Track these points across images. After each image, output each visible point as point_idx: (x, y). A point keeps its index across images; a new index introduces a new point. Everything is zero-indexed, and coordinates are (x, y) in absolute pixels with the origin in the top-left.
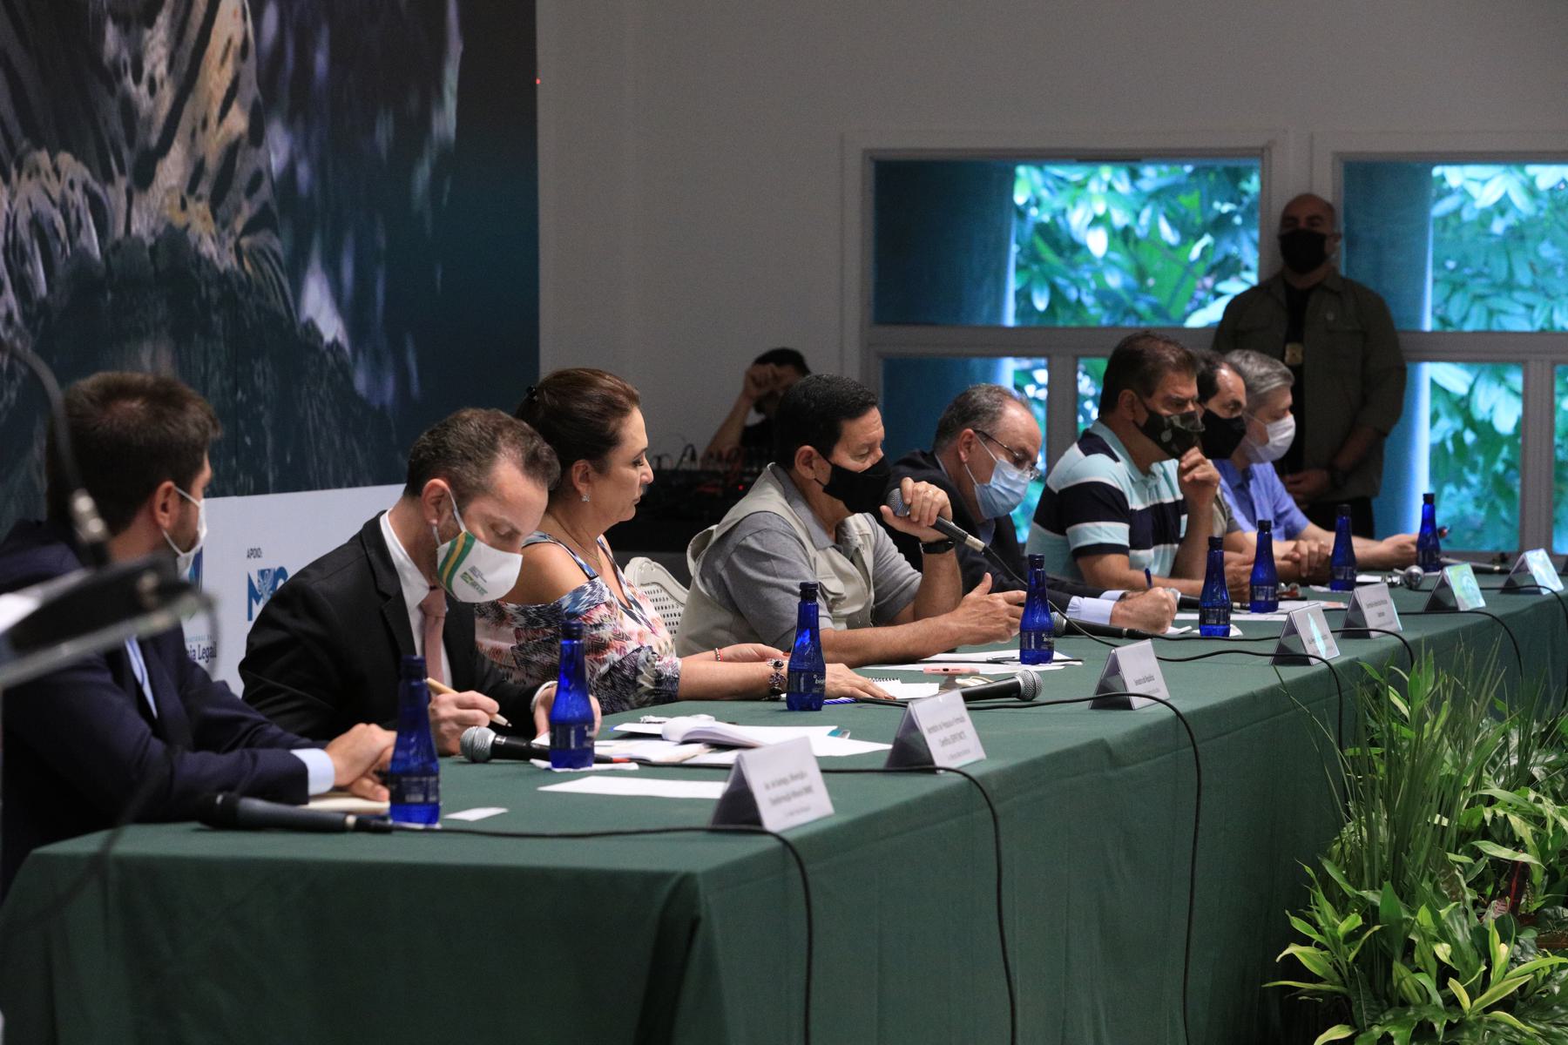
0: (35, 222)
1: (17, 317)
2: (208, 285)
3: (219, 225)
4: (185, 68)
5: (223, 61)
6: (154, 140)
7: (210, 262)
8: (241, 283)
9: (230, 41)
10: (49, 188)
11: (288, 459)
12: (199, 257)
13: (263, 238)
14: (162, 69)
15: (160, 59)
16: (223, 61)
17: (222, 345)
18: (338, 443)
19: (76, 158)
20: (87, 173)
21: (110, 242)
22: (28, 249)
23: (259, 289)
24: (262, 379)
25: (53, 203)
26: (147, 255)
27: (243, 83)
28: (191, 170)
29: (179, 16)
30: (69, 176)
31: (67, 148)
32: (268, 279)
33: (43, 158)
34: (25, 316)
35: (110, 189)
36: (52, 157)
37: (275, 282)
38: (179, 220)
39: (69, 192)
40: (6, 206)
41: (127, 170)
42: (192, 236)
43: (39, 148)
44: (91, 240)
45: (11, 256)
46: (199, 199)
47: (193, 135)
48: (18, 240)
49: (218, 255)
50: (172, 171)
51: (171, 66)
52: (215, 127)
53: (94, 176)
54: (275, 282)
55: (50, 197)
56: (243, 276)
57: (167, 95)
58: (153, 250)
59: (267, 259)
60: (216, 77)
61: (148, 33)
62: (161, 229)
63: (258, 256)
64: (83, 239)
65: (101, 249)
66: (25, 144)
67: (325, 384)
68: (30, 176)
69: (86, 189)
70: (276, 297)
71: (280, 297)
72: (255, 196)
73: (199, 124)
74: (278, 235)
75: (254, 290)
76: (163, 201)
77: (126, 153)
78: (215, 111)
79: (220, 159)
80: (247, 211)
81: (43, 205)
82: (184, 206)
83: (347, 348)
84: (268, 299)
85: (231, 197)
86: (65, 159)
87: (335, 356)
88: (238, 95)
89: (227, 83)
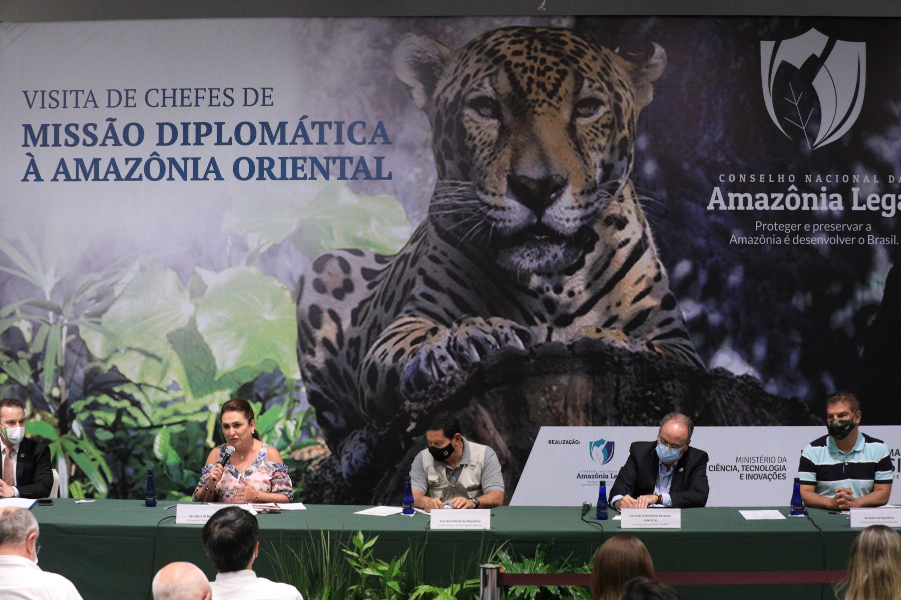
0: (472, 340)
1: (456, 366)
2: (620, 356)
3: (631, 337)
4: (602, 287)
5: (637, 283)
6: (572, 311)
7: (623, 349)
8: (651, 356)
9: (643, 276)
10: (483, 328)
11: (697, 415)
12: (612, 349)
13: (672, 341)
14: (582, 288)
15: (578, 285)
16: (637, 283)
17: (633, 376)
18: (746, 410)
19: (505, 318)
20: (514, 323)
21: (532, 344)
22: (466, 347)
23: (669, 358)
24: (671, 388)
25: (486, 333)
26: (566, 348)
27: (653, 289)
28: (605, 319)
29: (596, 271)
30: (499, 324)
31: (497, 316)
32: (678, 354)
33: (479, 320)
34: (463, 368)
35: (533, 328)
36: (485, 320)
37: (684, 354)
38: (594, 336)
39: (500, 330)
40: (449, 335)
41: (548, 321)
42: (606, 341)
43: (475, 315)
44: (520, 345)
45: (452, 349)
46: (614, 328)
47: (609, 308)
48: (458, 344)
49: (631, 347)
50: (592, 318)
51: (588, 286)
52: (628, 305)
53: (520, 324)
54: (684, 354)
55: (483, 331)
56: (655, 354)
57: (585, 297)
58: (570, 347)
59: (678, 347)
60: (629, 287)
61: (567, 278)
62: (578, 339)
63: (668, 346)
64: (511, 343)
65: (525, 346)
66: (464, 316)
67: (734, 390)
68: (467, 325)
69: (512, 328)
70: (686, 360)
71: (690, 360)
72: (666, 327)
73: (614, 304)
74: (688, 339)
75: (664, 358)
76: (579, 331)
77: (547, 316)
78: (630, 300)
79: (633, 315)
80: (658, 332)
81: (479, 335)
82: (598, 331)
83: (758, 376)
84: (678, 360)
85: (642, 328)
86: (496, 321)
87: (745, 381)
88: (651, 294)
89: (641, 290)
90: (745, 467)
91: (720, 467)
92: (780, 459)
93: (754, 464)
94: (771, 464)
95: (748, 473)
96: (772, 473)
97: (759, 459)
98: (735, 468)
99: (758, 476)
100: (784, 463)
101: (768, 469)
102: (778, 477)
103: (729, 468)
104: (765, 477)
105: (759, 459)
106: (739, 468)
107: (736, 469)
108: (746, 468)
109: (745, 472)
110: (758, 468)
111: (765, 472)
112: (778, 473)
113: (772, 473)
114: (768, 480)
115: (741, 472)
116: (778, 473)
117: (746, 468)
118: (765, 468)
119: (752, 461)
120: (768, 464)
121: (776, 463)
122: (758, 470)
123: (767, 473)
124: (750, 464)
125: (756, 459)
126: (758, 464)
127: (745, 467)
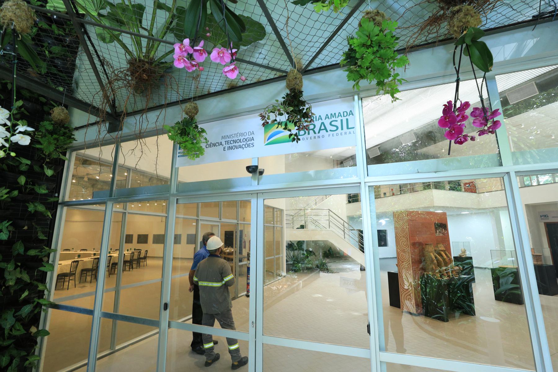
90: (227, 142)
91: (212, 145)
92: (250, 133)
93: (233, 139)
94: (244, 137)
95: (229, 145)
96: (245, 143)
97: (236, 135)
98: (221, 144)
99: (235, 146)
100: (253, 136)
101: (242, 141)
102: (249, 146)
103: (217, 144)
104: (240, 147)
105: (236, 135)
106: (224, 143)
107: (222, 144)
108: (227, 142)
109: (227, 146)
110: (235, 142)
111: (240, 143)
112: (248, 143)
113: (245, 143)
114: (242, 149)
115: (224, 146)
116: (249, 142)
117: (227, 142)
118: (240, 141)
119: (231, 137)
120: (242, 138)
121: (247, 136)
122: (235, 143)
123: (241, 144)
124: (230, 140)
125: (234, 135)
126: (235, 139)
127: (227, 142)
